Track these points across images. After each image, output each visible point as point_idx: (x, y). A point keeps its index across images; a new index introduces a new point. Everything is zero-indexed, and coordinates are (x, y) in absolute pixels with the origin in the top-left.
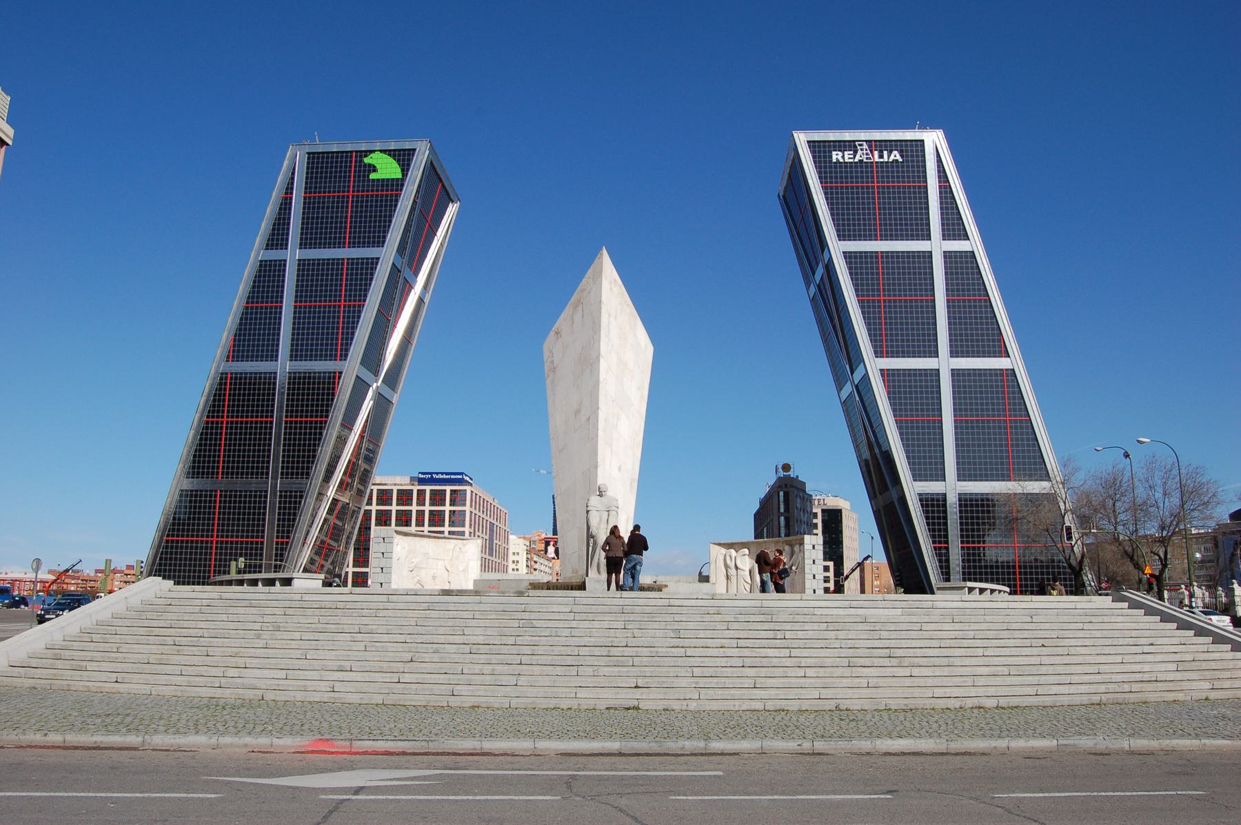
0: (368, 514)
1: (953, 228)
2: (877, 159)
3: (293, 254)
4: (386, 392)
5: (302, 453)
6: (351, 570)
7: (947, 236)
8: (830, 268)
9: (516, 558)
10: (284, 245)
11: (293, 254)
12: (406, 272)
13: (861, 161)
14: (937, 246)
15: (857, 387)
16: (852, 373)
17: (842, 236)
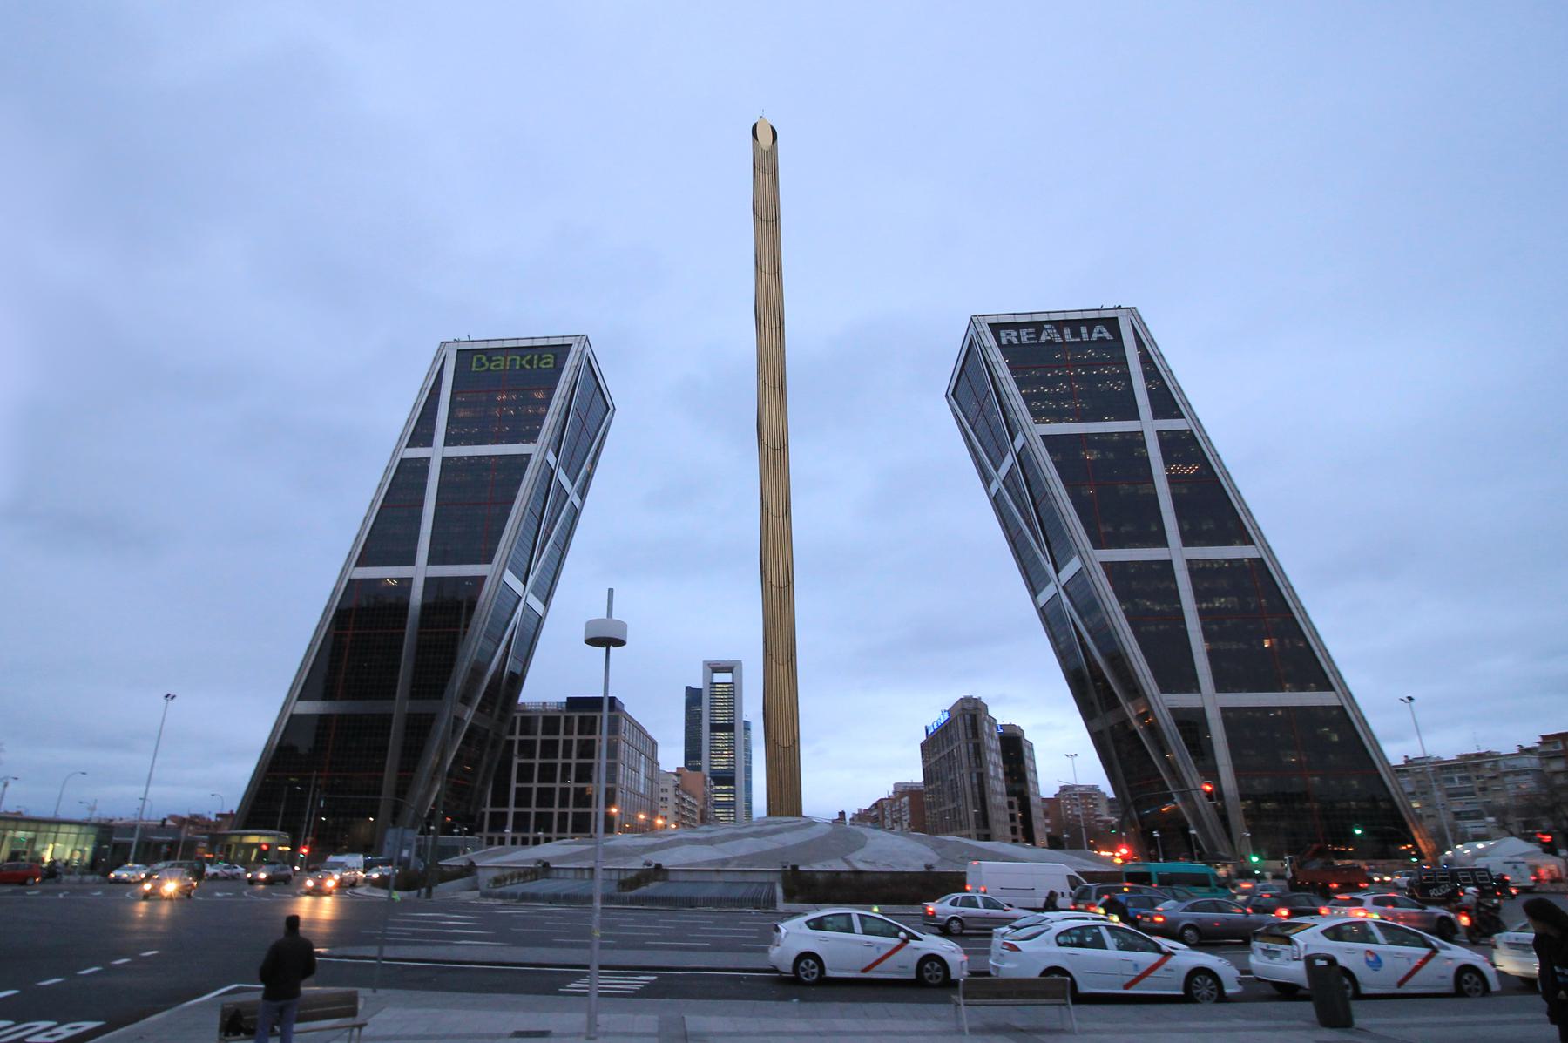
0: (511, 743)
1: (1166, 401)
2: (1068, 337)
3: (437, 452)
4: (538, 607)
5: (434, 672)
6: (488, 810)
7: (1158, 413)
8: (1023, 458)
9: (663, 795)
10: (429, 443)
11: (437, 452)
12: (562, 476)
13: (1049, 342)
14: (1148, 426)
15: (1064, 587)
16: (1057, 572)
17: (1037, 416)
